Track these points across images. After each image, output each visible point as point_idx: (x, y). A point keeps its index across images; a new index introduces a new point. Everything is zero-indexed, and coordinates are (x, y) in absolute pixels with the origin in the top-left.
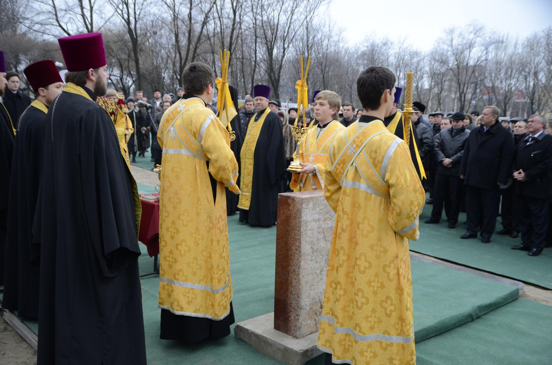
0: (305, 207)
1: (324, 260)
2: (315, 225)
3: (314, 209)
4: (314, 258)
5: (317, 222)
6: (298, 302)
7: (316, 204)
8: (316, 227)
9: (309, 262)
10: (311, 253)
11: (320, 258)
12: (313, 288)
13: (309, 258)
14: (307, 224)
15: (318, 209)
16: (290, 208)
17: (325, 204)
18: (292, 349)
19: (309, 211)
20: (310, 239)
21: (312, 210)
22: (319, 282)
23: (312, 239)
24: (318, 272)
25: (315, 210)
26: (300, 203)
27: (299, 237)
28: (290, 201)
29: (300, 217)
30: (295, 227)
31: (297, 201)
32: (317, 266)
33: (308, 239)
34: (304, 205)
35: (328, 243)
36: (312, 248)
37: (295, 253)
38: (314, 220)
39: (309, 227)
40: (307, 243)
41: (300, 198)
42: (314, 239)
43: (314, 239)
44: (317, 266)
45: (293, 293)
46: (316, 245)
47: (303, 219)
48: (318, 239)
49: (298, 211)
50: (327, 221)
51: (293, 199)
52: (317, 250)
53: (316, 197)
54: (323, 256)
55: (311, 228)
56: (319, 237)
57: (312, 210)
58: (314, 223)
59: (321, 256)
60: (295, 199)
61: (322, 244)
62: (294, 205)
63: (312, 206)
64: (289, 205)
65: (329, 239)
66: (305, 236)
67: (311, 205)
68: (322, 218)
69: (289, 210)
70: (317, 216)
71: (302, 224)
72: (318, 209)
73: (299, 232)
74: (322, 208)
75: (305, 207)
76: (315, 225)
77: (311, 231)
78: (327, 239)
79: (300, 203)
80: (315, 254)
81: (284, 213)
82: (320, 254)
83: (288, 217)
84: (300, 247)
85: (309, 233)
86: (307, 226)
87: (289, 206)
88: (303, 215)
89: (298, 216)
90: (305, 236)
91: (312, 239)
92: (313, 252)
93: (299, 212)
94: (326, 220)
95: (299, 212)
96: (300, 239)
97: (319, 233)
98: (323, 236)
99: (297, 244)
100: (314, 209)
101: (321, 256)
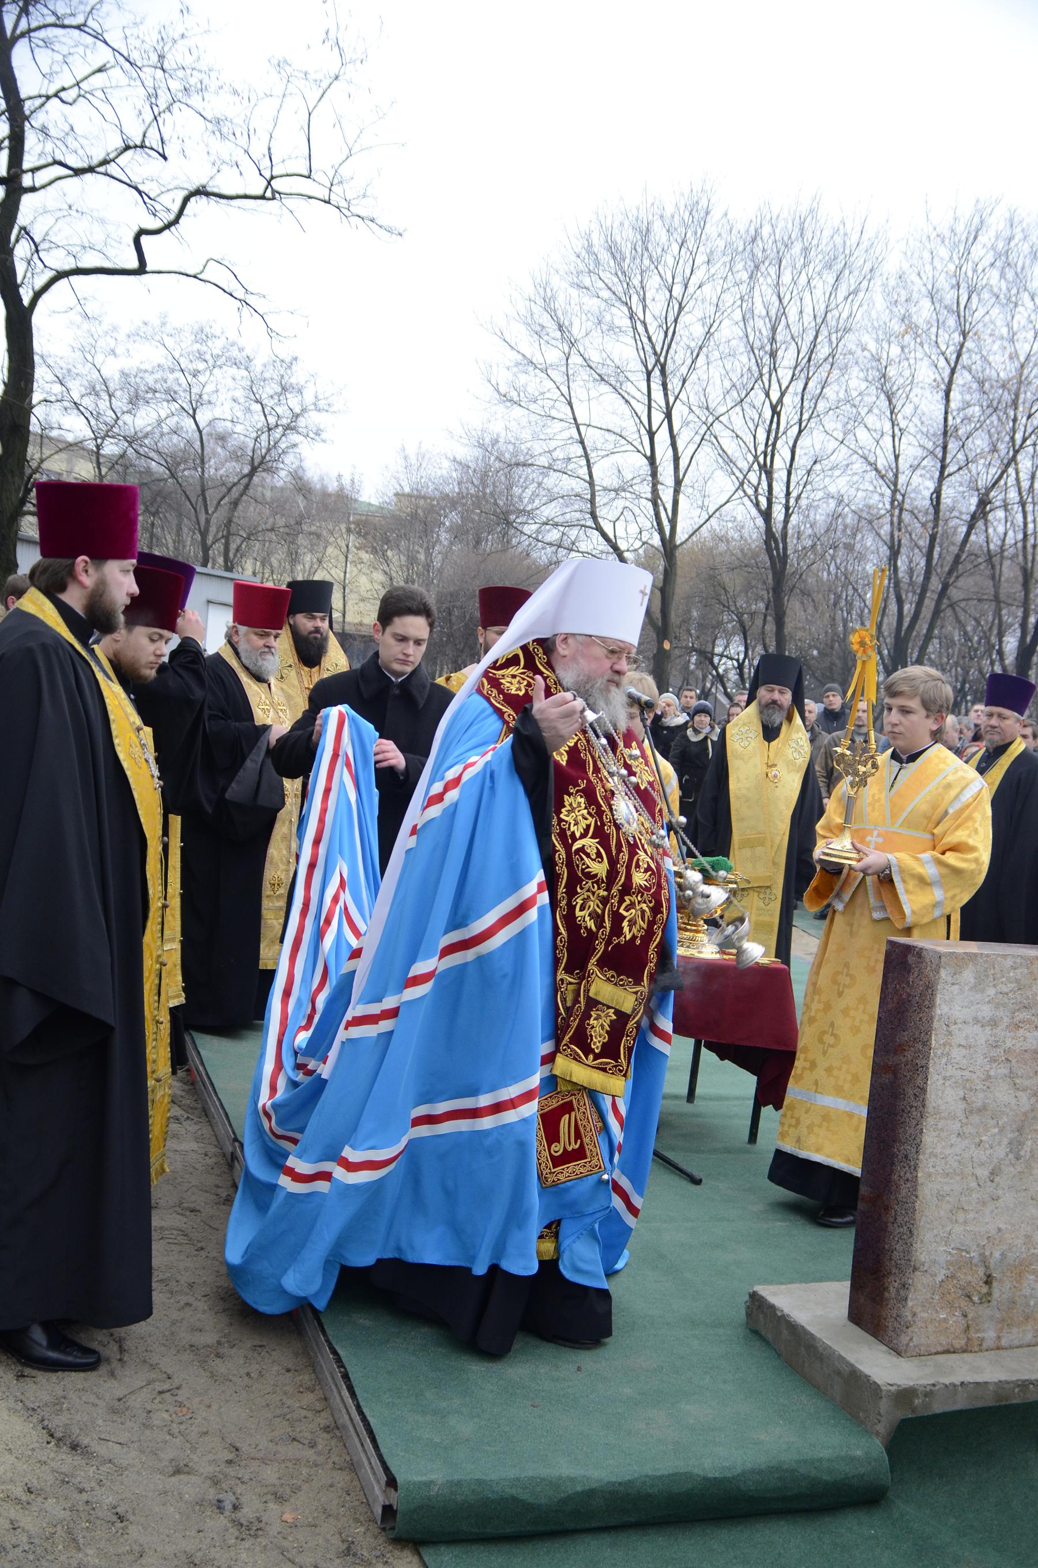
1: (1005, 1141)
2: (982, 1036)
3: (978, 986)
4: (969, 1130)
6: (908, 1250)
7: (987, 976)
9: (954, 1139)
10: (960, 1114)
11: (995, 1135)
12: (961, 1216)
13: (956, 1126)
15: (992, 992)
17: (1017, 981)
18: (867, 1377)
19: (962, 991)
20: (960, 1073)
21: (971, 989)
23: (966, 1073)
24: (983, 1173)
25: (983, 991)
26: (934, 966)
27: (924, 1062)
28: (911, 959)
29: (931, 1006)
30: (917, 1035)
32: (980, 1155)
33: (950, 1071)
34: (943, 973)
36: (964, 1098)
37: (911, 1107)
38: (976, 1021)
39: (959, 1038)
40: (948, 1083)
42: (974, 1076)
43: (974, 1076)
44: (980, 1155)
45: (900, 1219)
46: (981, 1095)
47: (938, 1012)
48: (989, 1077)
49: (928, 987)
50: (1021, 1030)
52: (984, 1108)
53: (988, 956)
54: (1002, 1130)
55: (963, 1043)
56: (992, 1073)
57: (971, 989)
58: (977, 1028)
59: (996, 1130)
60: (924, 953)
61: (1003, 1094)
62: (920, 973)
63: (972, 980)
65: (1027, 1083)
66: (944, 1060)
67: (968, 975)
68: (1006, 1020)
70: (986, 1011)
71: (936, 1025)
73: (926, 1049)
74: (1005, 990)
75: (949, 979)
76: (982, 1036)
77: (964, 1051)
78: (1018, 1081)
79: (934, 966)
80: (975, 1119)
81: (896, 992)
82: (993, 1122)
83: (904, 1003)
84: (924, 1090)
85: (957, 1054)
86: (950, 1033)
87: (909, 972)
88: (938, 1001)
89: (927, 1003)
90: (944, 1060)
91: (966, 1073)
92: (969, 1112)
93: (930, 988)
94: (1017, 1027)
95: (930, 991)
96: (928, 1068)
97: (993, 1060)
98: (1006, 1071)
99: (919, 1081)
100: (978, 986)
101: (996, 1130)
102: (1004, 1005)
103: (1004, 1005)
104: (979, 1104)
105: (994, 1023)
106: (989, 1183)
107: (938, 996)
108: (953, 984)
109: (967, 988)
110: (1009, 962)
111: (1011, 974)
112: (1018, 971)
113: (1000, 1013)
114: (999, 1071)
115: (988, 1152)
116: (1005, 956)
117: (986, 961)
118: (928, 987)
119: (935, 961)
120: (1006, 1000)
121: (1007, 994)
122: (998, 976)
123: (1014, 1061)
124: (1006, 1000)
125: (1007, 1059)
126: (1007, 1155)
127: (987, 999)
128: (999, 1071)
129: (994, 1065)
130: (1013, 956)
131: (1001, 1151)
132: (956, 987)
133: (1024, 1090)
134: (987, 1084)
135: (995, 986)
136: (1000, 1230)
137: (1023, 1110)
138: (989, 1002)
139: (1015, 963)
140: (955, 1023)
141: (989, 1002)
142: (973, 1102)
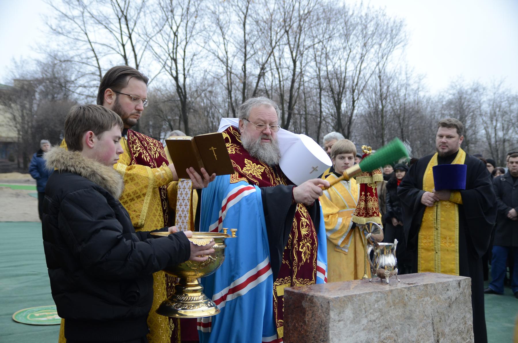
0: (337, 318)
3: (356, 320)
7: (361, 311)
15: (364, 321)
16: (307, 320)
17: (380, 310)
21: (351, 322)
25: (359, 322)
26: (324, 310)
28: (305, 304)
31: (319, 305)
34: (332, 314)
41: (324, 298)
49: (321, 325)
51: (311, 300)
53: (360, 295)
57: (351, 322)
63: (351, 316)
64: (304, 312)
67: (348, 312)
69: (304, 322)
72: (364, 321)
74: (373, 318)
75: (337, 318)
79: (324, 310)
87: (304, 314)
88: (331, 336)
89: (321, 337)
95: (323, 329)
100: (356, 320)
102: (373, 329)
103: (373, 329)
107: (331, 332)
108: (339, 321)
109: (348, 322)
110: (373, 298)
111: (376, 306)
112: (380, 303)
113: (371, 336)
116: (370, 294)
118: (321, 325)
119: (325, 306)
120: (374, 326)
122: (368, 309)
124: (374, 326)
127: (362, 328)
130: (376, 293)
132: (342, 323)
135: (366, 317)
138: (364, 329)
139: (377, 297)
141: (364, 329)
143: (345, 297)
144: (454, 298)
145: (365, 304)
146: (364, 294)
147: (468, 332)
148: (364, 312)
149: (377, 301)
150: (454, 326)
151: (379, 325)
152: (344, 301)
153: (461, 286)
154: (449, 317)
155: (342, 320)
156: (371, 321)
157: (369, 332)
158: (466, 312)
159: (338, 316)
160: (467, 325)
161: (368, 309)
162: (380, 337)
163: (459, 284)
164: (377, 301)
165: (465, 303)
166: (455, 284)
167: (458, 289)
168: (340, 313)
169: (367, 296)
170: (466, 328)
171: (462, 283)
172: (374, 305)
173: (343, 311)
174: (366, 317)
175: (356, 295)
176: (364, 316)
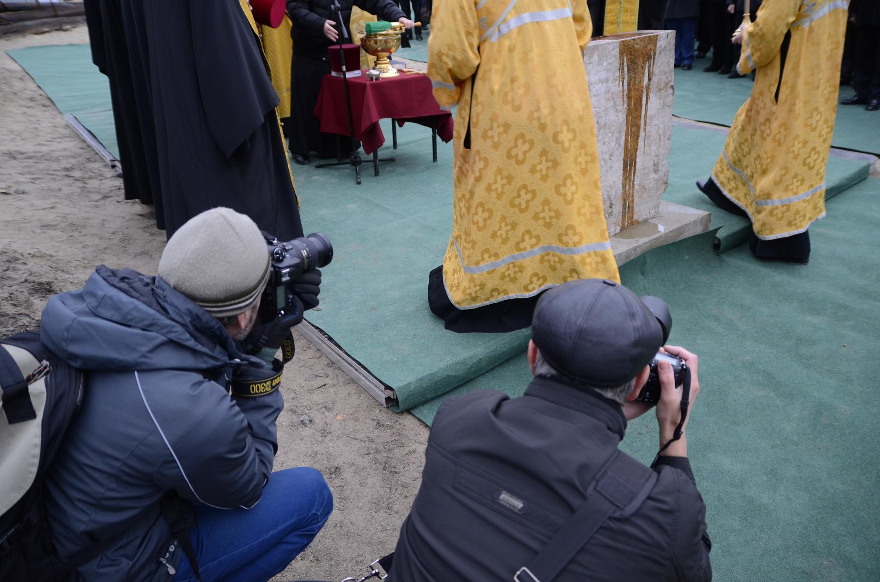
3: (600, 63)
5: (605, 84)
7: (603, 56)
8: (603, 91)
11: (610, 137)
14: (591, 87)
15: (605, 64)
20: (595, 110)
22: (607, 171)
23: (598, 109)
24: (607, 157)
25: (602, 65)
32: (605, 148)
35: (619, 114)
36: (598, 122)
38: (600, 81)
43: (601, 110)
44: (605, 148)
46: (604, 119)
48: (607, 109)
52: (605, 125)
53: (603, 45)
54: (613, 134)
56: (608, 106)
57: (597, 65)
58: (600, 85)
59: (610, 135)
68: (612, 77)
70: (603, 75)
72: (605, 64)
74: (611, 62)
78: (617, 108)
80: (602, 131)
82: (609, 131)
91: (598, 109)
97: (608, 100)
100: (600, 63)
101: (610, 135)
104: (603, 124)
105: (607, 80)
106: (609, 161)
108: (590, 64)
109: (595, 64)
111: (613, 53)
112: (615, 50)
114: (611, 104)
115: (608, 146)
117: (602, 48)
121: (611, 64)
123: (616, 99)
124: (611, 67)
125: (613, 98)
126: (615, 145)
127: (604, 69)
128: (611, 104)
129: (608, 102)
131: (613, 144)
133: (620, 112)
134: (606, 112)
135: (606, 61)
136: (614, 182)
137: (620, 121)
138: (605, 70)
139: (614, 46)
140: (592, 84)
141: (605, 70)
142: (601, 123)
143: (594, 46)
144: (663, 47)
145: (606, 51)
146: (605, 44)
147: (670, 72)
148: (605, 57)
149: (613, 49)
150: (662, 68)
151: (614, 67)
152: (593, 49)
153: (669, 36)
154: (659, 61)
155: (591, 63)
156: (609, 64)
157: (608, 72)
158: (670, 57)
159: (589, 60)
160: (670, 68)
161: (608, 55)
162: (614, 76)
163: (668, 35)
164: (613, 49)
165: (670, 51)
166: (665, 36)
167: (666, 40)
168: (590, 58)
169: (607, 45)
170: (670, 70)
171: (669, 35)
172: (611, 52)
173: (592, 56)
174: (606, 61)
175: (600, 45)
176: (605, 60)
